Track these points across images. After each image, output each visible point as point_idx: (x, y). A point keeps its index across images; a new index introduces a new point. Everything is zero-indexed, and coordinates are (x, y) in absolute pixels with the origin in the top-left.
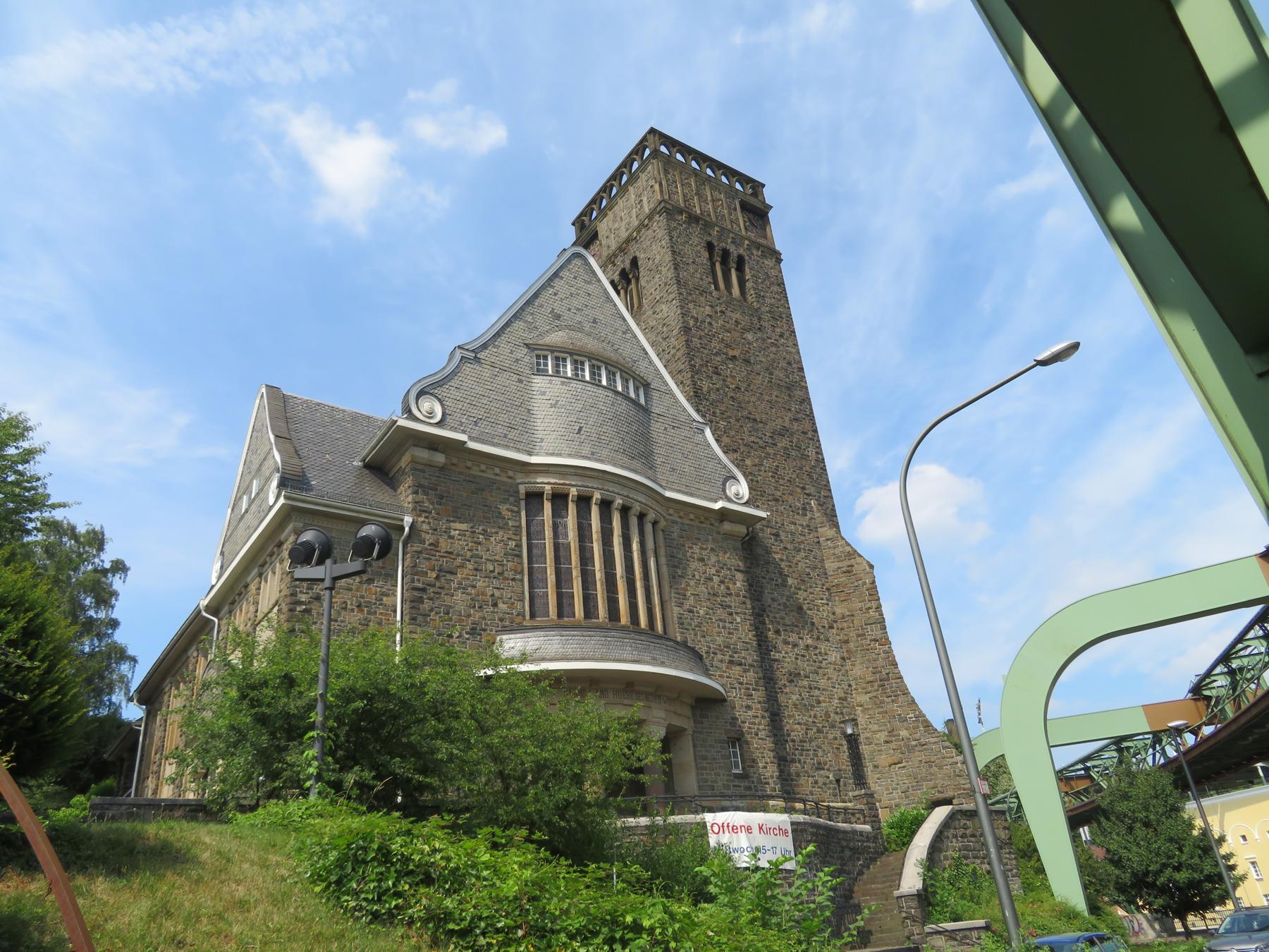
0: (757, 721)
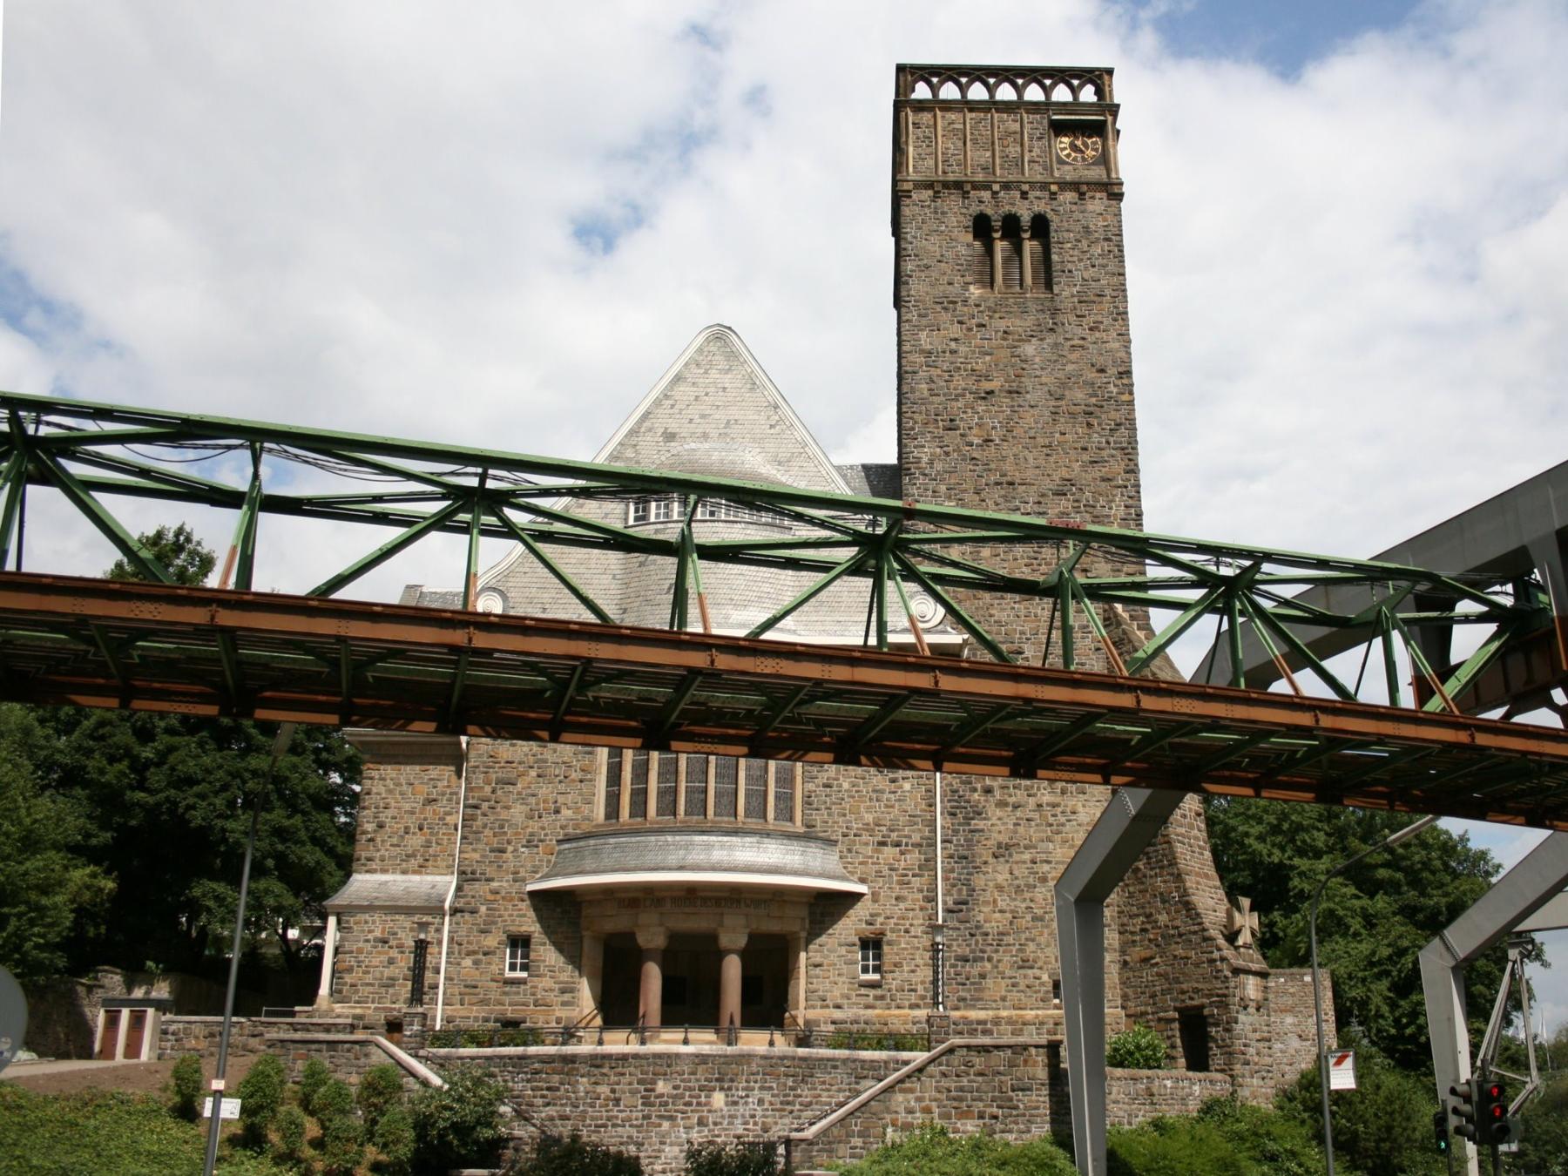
0: (911, 914)
